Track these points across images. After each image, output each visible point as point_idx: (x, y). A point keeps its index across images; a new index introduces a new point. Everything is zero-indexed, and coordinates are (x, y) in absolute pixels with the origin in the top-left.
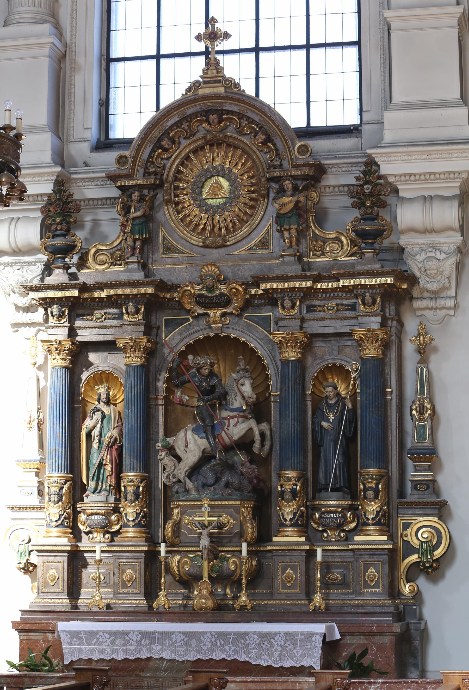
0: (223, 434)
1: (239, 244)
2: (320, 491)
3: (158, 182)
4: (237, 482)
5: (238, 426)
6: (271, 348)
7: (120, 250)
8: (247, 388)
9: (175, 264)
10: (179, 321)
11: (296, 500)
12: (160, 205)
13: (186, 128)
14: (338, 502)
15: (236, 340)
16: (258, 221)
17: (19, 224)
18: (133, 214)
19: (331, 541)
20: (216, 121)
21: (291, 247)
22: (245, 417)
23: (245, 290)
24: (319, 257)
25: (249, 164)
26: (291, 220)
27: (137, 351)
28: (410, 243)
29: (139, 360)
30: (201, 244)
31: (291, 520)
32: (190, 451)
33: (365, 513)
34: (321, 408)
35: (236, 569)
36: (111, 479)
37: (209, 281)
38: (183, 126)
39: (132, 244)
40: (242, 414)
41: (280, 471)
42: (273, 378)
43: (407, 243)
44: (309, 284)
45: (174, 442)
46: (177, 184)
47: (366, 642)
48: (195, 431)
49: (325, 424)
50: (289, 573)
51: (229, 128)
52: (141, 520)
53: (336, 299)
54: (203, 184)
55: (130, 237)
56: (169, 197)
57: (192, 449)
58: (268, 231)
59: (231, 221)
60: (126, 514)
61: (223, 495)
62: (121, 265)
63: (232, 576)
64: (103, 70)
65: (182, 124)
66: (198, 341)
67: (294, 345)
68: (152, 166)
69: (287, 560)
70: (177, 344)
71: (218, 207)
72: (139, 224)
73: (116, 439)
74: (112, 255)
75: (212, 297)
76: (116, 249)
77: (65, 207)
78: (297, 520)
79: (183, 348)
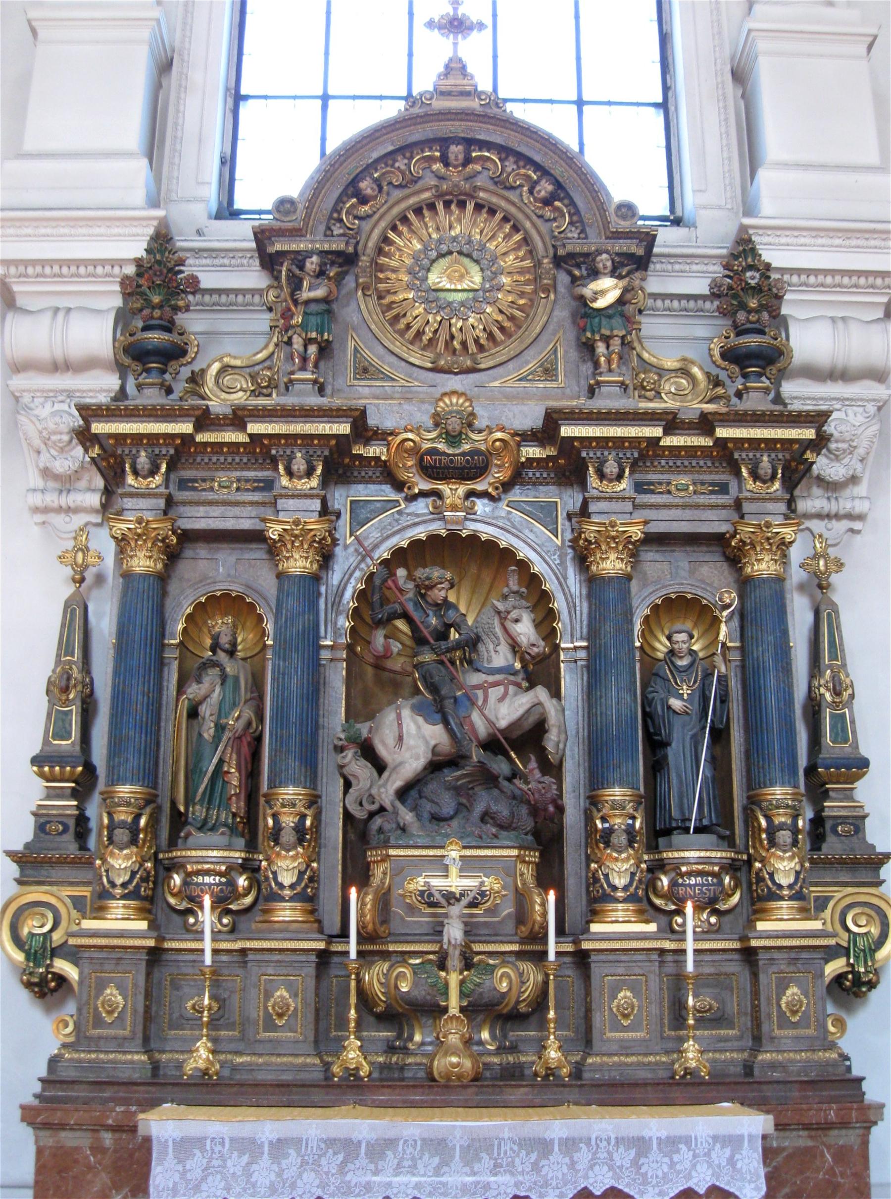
0: (476, 717)
1: (500, 370)
2: (667, 832)
3: (351, 249)
4: (506, 813)
5: (507, 700)
6: (557, 562)
8: (525, 629)
9: (378, 398)
10: (378, 505)
11: (633, 847)
12: (352, 294)
13: (403, 167)
14: (703, 854)
15: (491, 545)
16: (538, 330)
17: (73, 315)
18: (305, 294)
20: (461, 157)
21: (610, 370)
22: (518, 685)
23: (519, 445)
24: (651, 400)
25: (518, 237)
26: (613, 321)
27: (306, 546)
28: (800, 394)
29: (308, 565)
30: (429, 365)
31: (625, 888)
32: (409, 749)
33: (771, 875)
34: (661, 674)
35: (510, 989)
36: (237, 803)
37: (454, 424)
38: (397, 165)
39: (301, 349)
40: (512, 678)
41: (594, 790)
43: (795, 394)
44: (657, 432)
45: (370, 732)
46: (383, 260)
47: (810, 1143)
48: (418, 710)
49: (676, 704)
50: (625, 997)
51: (480, 176)
52: (306, 886)
53: (691, 472)
54: (431, 265)
55: (300, 335)
56: (368, 280)
57: (412, 742)
58: (555, 351)
59: (485, 329)
60: (275, 873)
61: (481, 837)
62: (270, 395)
63: (498, 1004)
64: (228, 111)
65: (395, 161)
66: (416, 544)
67: (621, 548)
68: (338, 225)
69: (620, 970)
70: (376, 546)
71: (462, 304)
72: (318, 314)
73: (249, 724)
74: (253, 377)
75: (454, 455)
76: (261, 366)
77: (171, 279)
78: (637, 888)
79: (386, 555)
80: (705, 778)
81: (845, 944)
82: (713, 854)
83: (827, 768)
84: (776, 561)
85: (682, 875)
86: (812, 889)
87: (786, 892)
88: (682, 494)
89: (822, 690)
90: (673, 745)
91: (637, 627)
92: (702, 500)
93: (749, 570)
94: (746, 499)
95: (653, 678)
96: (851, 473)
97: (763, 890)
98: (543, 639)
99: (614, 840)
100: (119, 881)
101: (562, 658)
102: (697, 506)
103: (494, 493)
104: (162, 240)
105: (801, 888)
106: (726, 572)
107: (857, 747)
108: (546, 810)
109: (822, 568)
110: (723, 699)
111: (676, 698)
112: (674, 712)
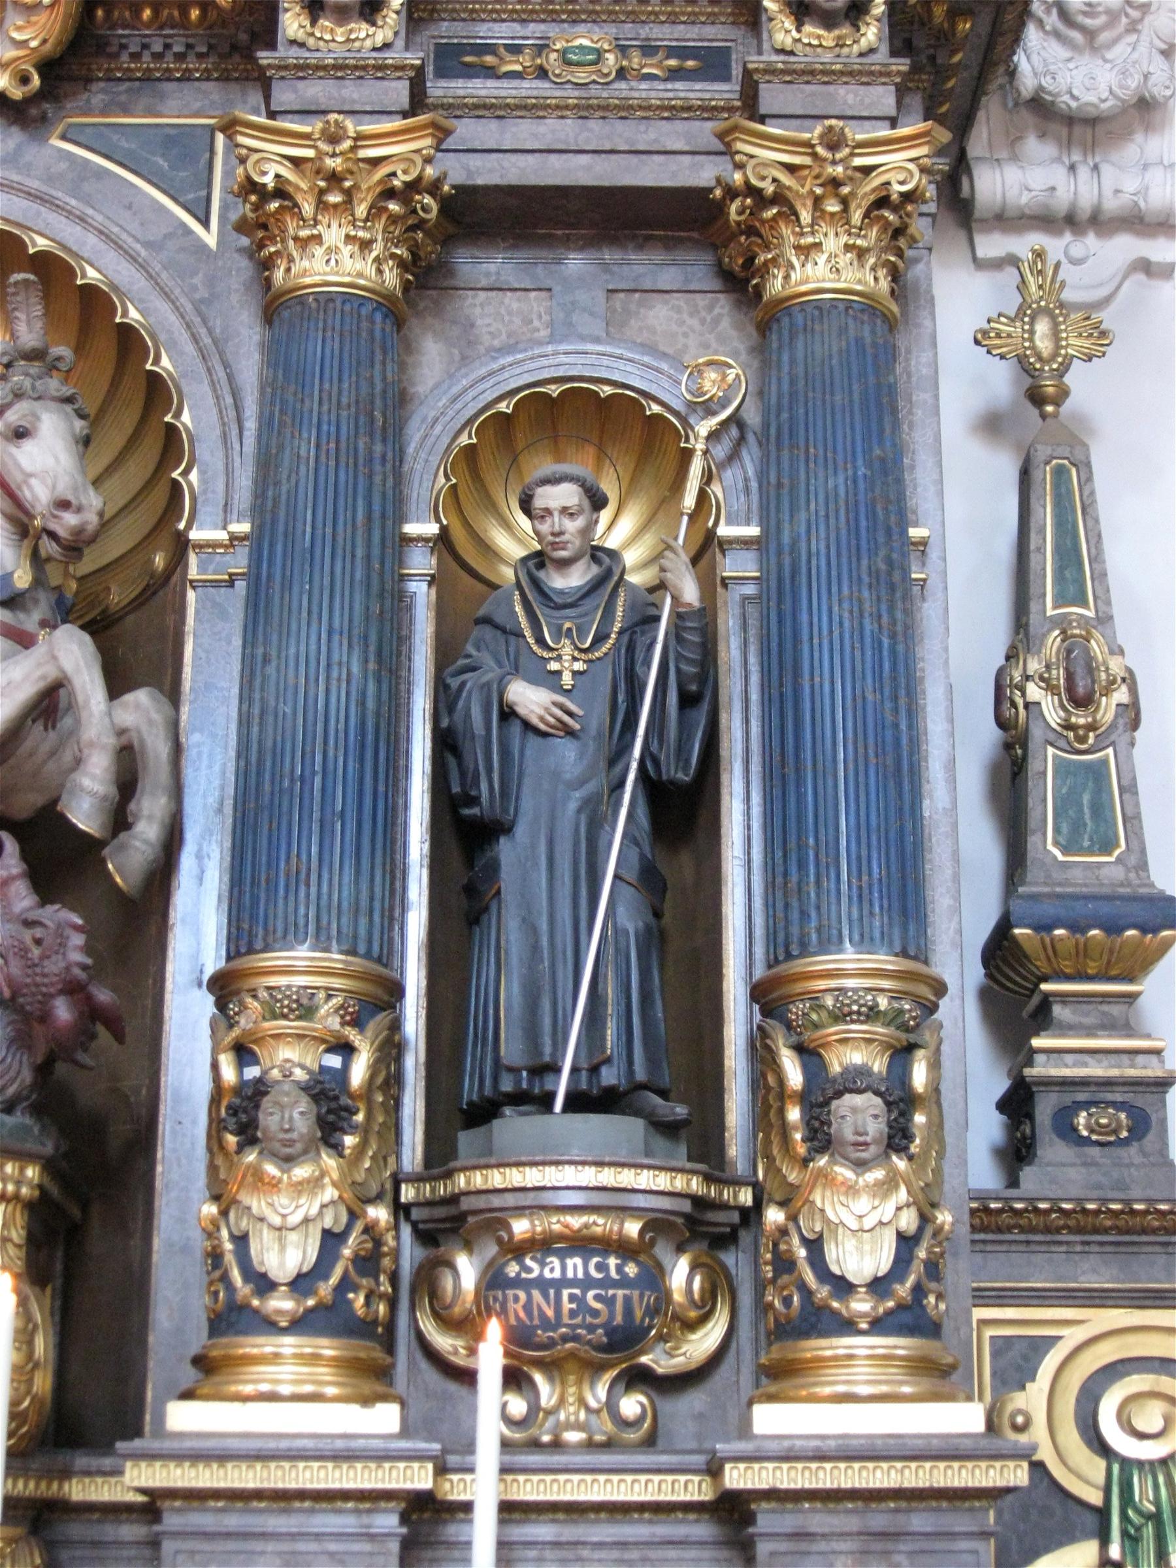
2: (482, 1113)
19: (557, 1445)
31: (301, 1283)
33: (815, 1246)
34: (499, 619)
42: (202, 452)
49: (530, 699)
78: (345, 1285)
80: (613, 937)
81: (1095, 1497)
82: (626, 1178)
83: (1043, 927)
84: (861, 253)
85: (518, 1250)
86: (980, 1313)
87: (861, 1305)
88: (582, 76)
89: (1034, 692)
90: (521, 830)
91: (428, 476)
92: (641, 91)
93: (776, 286)
94: (770, 71)
95: (477, 632)
96: (1133, 83)
97: (787, 1301)
98: (97, 483)
99: (270, 1119)
101: (193, 572)
102: (625, 110)
103: (17, 93)
105: (919, 1291)
106: (725, 324)
107: (1143, 865)
108: (45, 1017)
109: (1044, 345)
110: (697, 693)
111: (534, 681)
112: (527, 726)
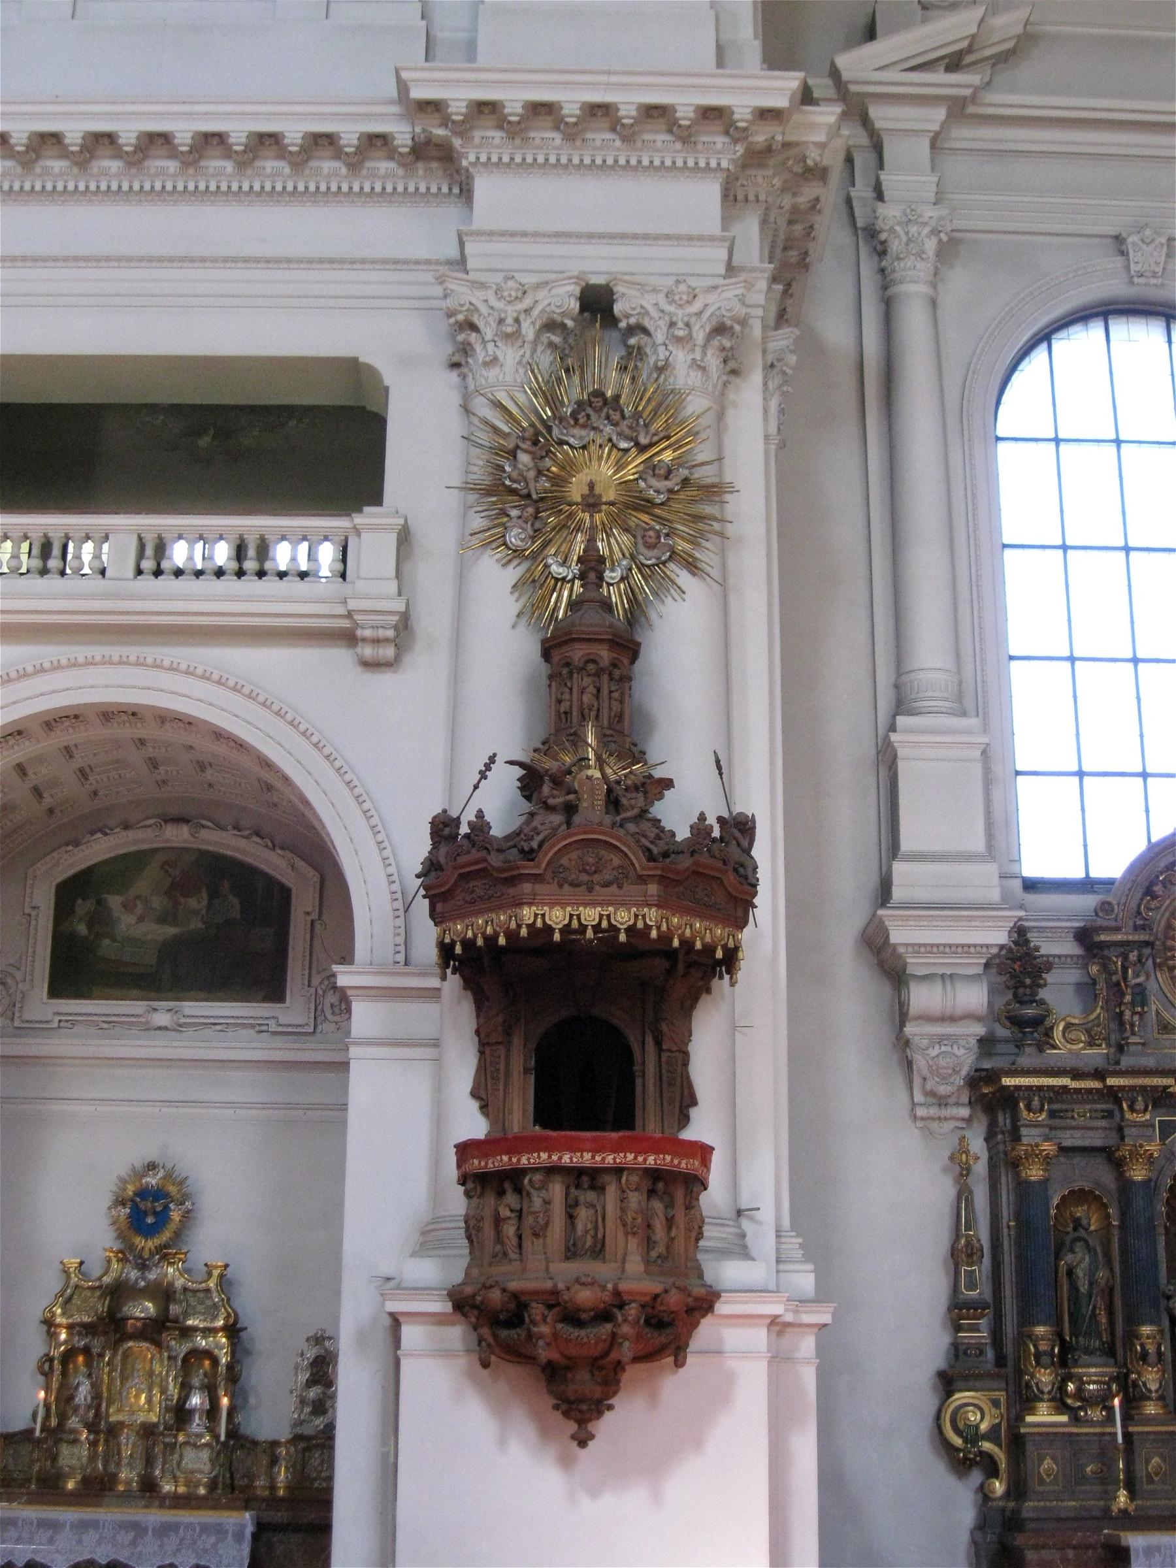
7: (1098, 1025)
60: (1145, 1384)
62: (1100, 1045)
74: (1088, 1031)
100: (1046, 1390)
104: (1020, 933)
